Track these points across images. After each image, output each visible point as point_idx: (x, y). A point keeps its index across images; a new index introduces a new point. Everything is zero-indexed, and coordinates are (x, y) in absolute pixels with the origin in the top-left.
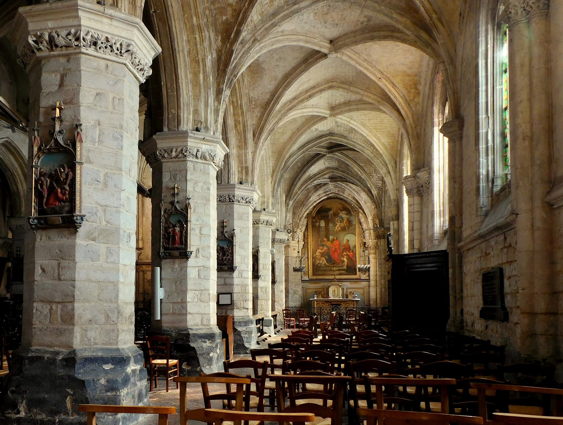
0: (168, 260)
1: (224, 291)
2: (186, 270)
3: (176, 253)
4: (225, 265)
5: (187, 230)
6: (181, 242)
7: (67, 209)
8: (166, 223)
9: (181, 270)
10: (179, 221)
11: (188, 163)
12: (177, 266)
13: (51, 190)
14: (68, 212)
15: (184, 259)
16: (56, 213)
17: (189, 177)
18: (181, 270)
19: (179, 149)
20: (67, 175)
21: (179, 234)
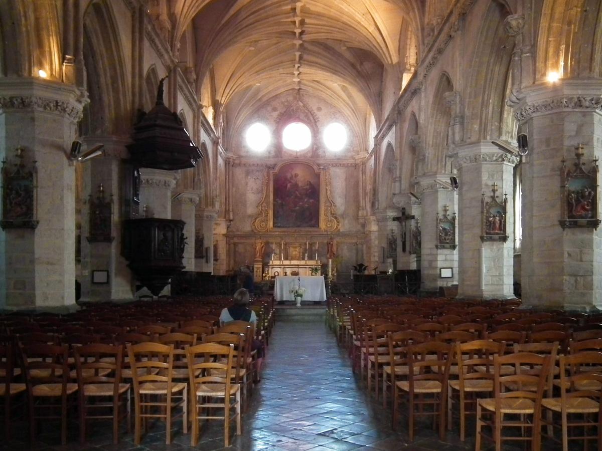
0: (488, 243)
1: (445, 266)
2: (503, 251)
3: (497, 237)
4: (447, 243)
5: (505, 219)
6: (500, 229)
7: (590, 215)
8: (487, 213)
9: (498, 250)
10: (498, 212)
11: (504, 166)
12: (495, 247)
13: (578, 201)
14: (592, 217)
15: (501, 242)
16: (582, 218)
17: (504, 177)
18: (498, 250)
19: (499, 155)
20: (590, 193)
21: (498, 222)
